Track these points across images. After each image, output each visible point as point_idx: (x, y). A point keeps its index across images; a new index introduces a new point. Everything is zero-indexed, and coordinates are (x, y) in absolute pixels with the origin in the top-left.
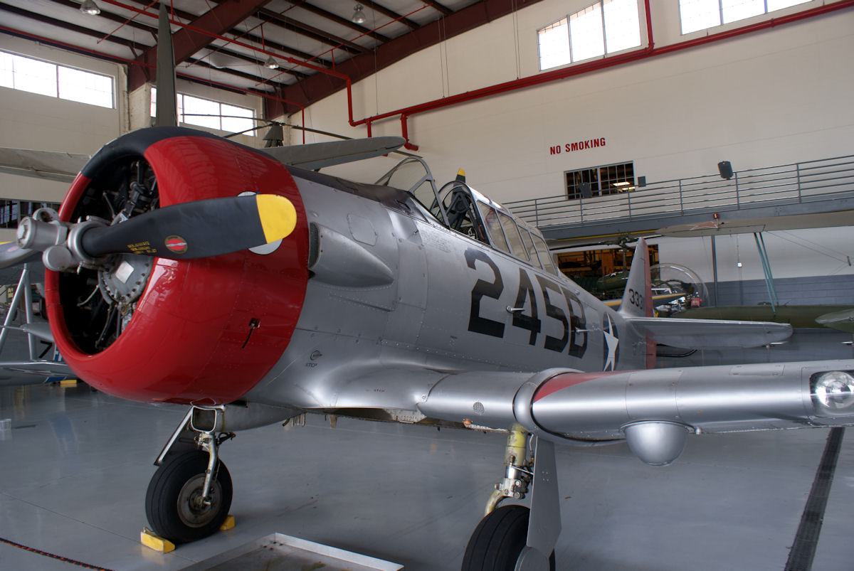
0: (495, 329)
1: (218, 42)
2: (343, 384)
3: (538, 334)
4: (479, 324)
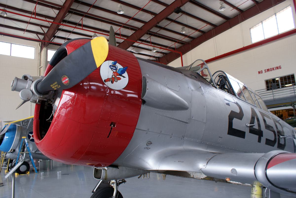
0: (241, 134)
1: (136, 44)
2: (163, 158)
3: (262, 137)
4: (232, 131)
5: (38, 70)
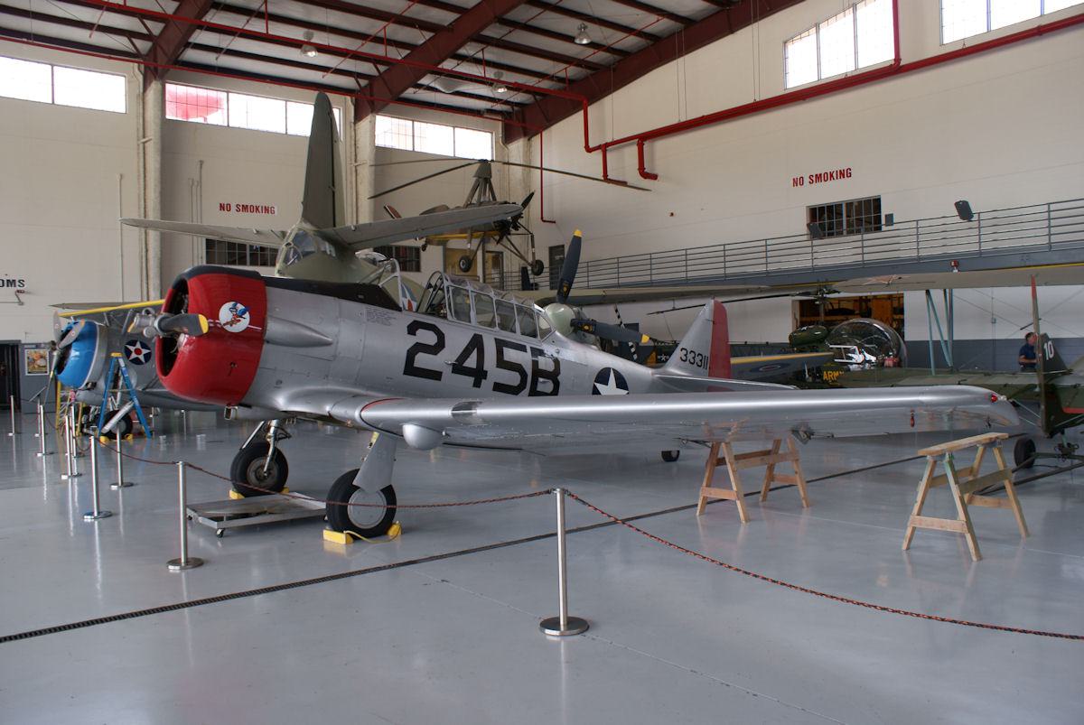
2: (294, 399)
3: (483, 381)
5: (138, 149)
